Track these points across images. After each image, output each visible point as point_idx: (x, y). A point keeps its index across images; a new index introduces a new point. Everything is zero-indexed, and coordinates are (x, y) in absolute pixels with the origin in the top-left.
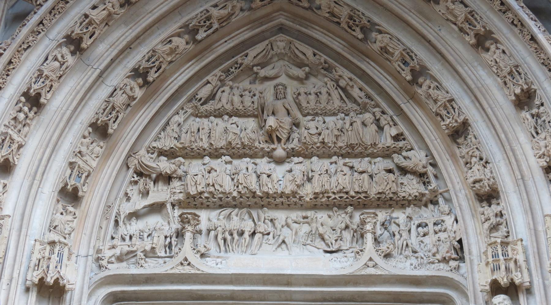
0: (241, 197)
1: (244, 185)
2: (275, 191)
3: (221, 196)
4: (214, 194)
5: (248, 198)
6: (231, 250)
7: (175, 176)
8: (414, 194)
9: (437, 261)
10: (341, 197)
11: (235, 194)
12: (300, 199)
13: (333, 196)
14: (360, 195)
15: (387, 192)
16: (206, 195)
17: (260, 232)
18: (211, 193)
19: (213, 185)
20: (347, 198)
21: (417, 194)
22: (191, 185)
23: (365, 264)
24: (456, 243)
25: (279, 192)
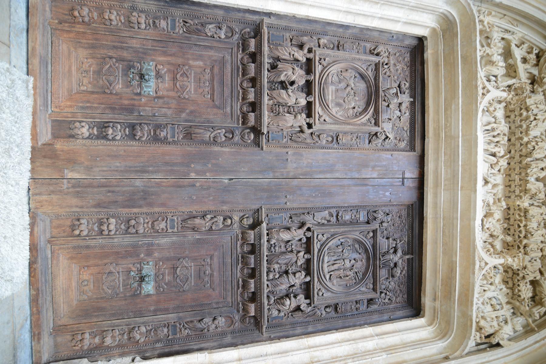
0: (521, 145)
1: (536, 147)
2: (531, 174)
3: (525, 126)
4: (526, 120)
5: (521, 151)
6: (485, 135)
7: (535, 87)
8: (522, 295)
9: (477, 321)
10: (520, 232)
11: (526, 139)
12: (516, 196)
13: (522, 225)
14: (522, 248)
15: (524, 272)
16: (525, 114)
17: (498, 161)
18: (527, 118)
19: (535, 119)
20: (519, 237)
21: (522, 298)
22: (535, 100)
23: (483, 259)
24: (497, 341)
25: (529, 178)
